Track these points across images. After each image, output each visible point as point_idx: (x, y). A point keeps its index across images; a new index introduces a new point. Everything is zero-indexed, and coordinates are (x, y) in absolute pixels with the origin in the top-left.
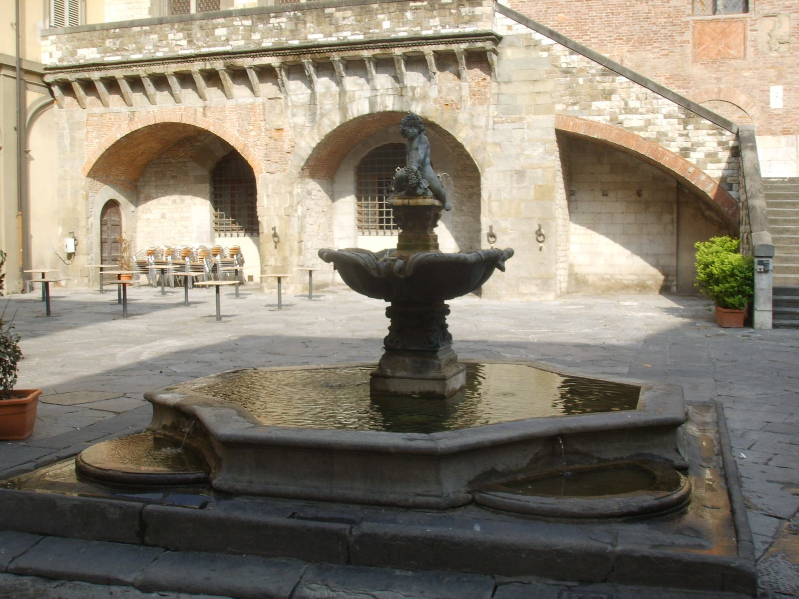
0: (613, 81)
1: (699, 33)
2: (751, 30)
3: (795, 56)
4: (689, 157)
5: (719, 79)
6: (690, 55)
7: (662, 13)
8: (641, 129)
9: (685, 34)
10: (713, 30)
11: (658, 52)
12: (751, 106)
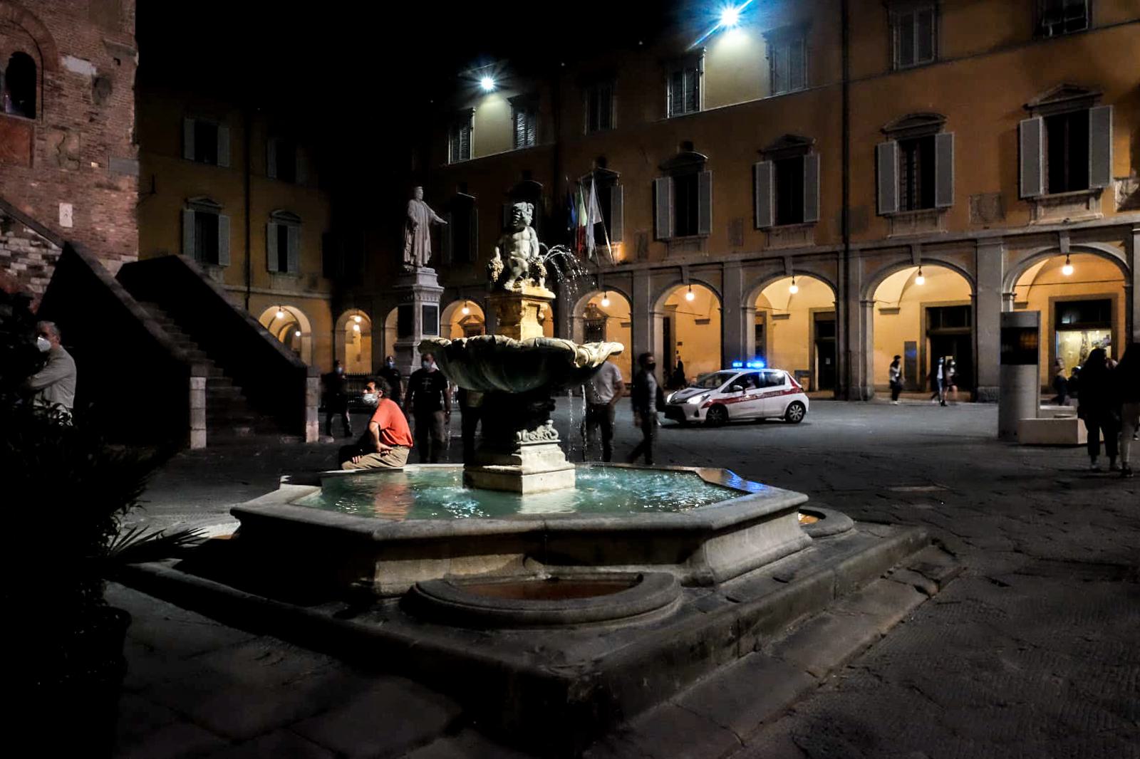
2: (39, 139)
4: (9, 267)
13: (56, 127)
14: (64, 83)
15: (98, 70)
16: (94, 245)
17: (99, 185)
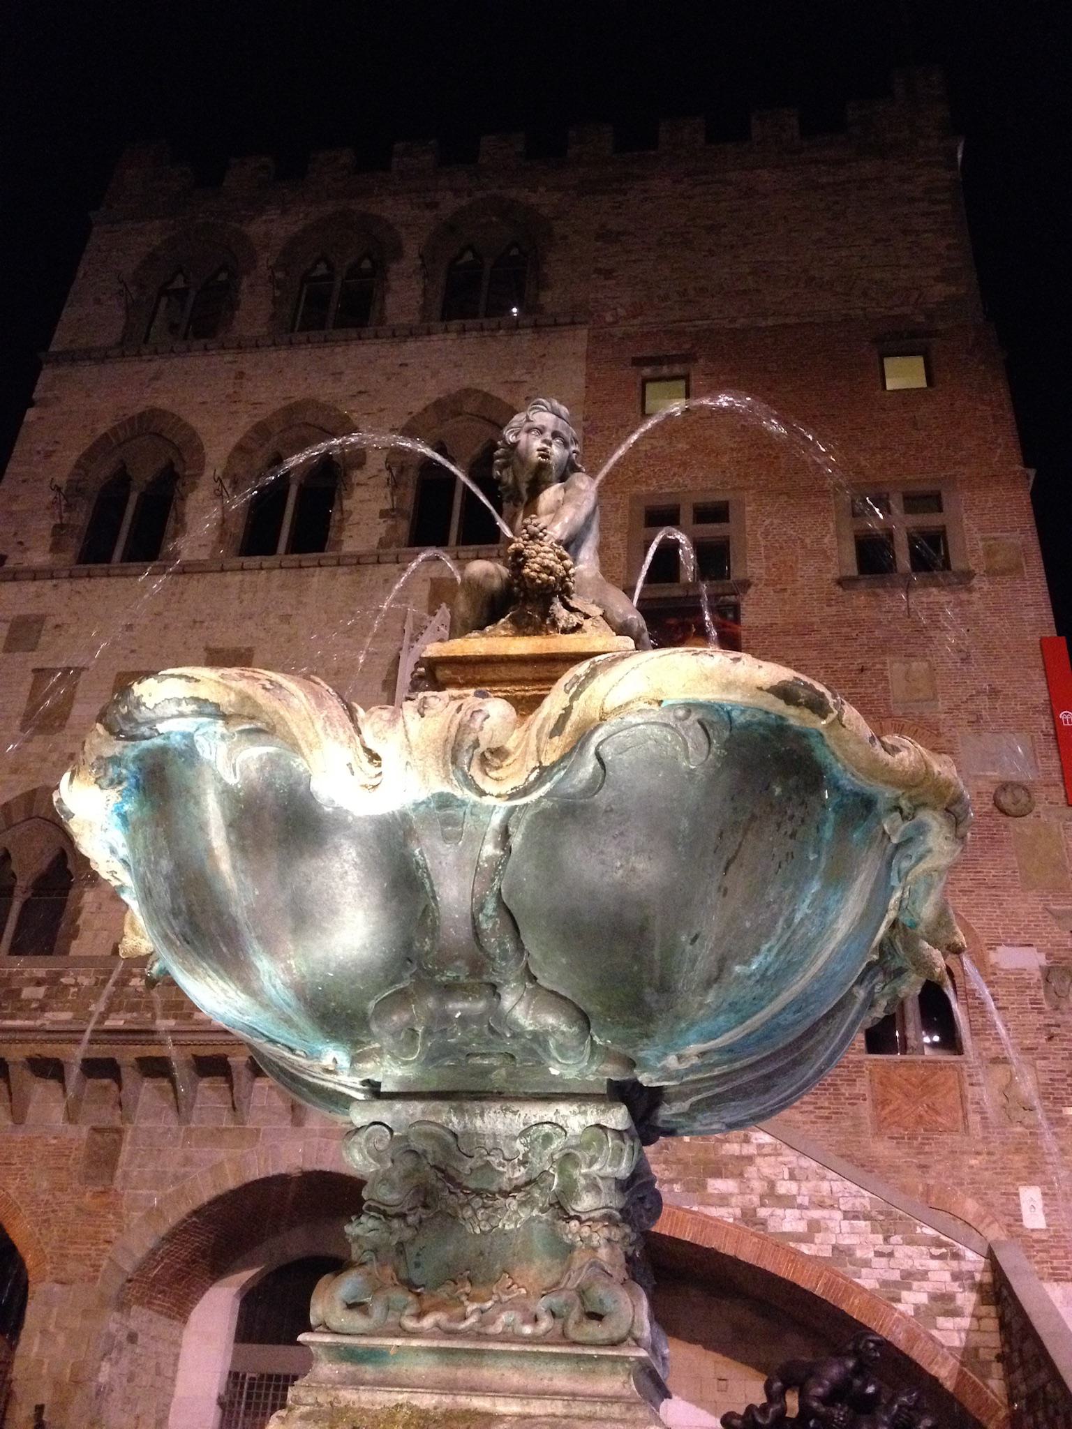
0: (747, 1140)
2: (972, 1084)
4: (899, 1300)
6: (868, 1121)
8: (800, 1238)
11: (811, 1112)
12: (987, 1221)
15: (1048, 956)
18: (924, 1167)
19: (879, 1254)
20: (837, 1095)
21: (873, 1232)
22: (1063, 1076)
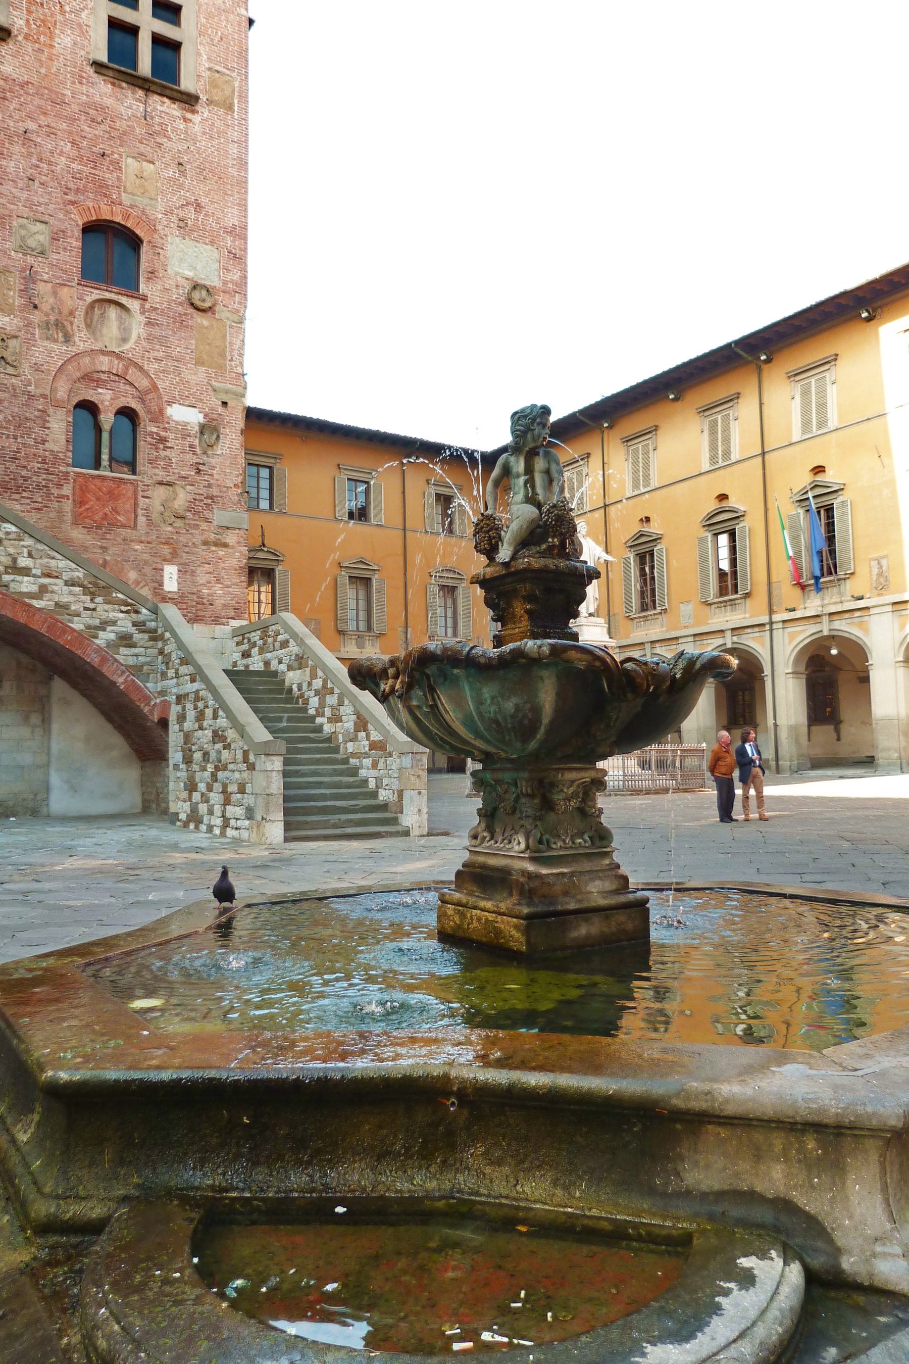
1: (81, 489)
2: (143, 497)
3: (191, 534)
4: (96, 637)
5: (104, 549)
7: (35, 455)
9: (65, 488)
10: (99, 489)
11: (28, 504)
12: (142, 585)
13: (161, 483)
14: (172, 436)
15: (206, 416)
16: (200, 610)
17: (206, 543)
18: (105, 548)
19: (86, 609)
20: (49, 495)
21: (84, 594)
22: (202, 498)
